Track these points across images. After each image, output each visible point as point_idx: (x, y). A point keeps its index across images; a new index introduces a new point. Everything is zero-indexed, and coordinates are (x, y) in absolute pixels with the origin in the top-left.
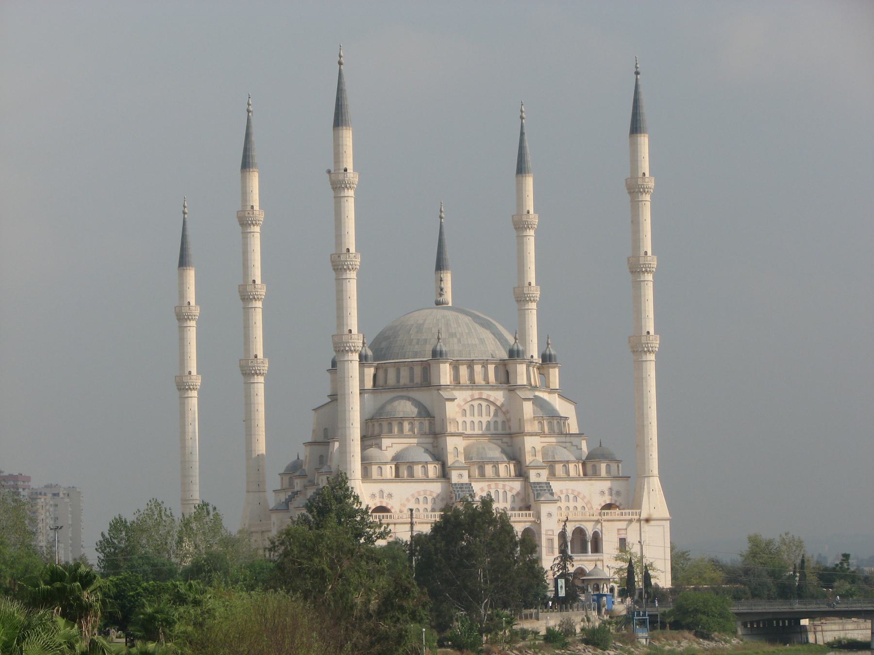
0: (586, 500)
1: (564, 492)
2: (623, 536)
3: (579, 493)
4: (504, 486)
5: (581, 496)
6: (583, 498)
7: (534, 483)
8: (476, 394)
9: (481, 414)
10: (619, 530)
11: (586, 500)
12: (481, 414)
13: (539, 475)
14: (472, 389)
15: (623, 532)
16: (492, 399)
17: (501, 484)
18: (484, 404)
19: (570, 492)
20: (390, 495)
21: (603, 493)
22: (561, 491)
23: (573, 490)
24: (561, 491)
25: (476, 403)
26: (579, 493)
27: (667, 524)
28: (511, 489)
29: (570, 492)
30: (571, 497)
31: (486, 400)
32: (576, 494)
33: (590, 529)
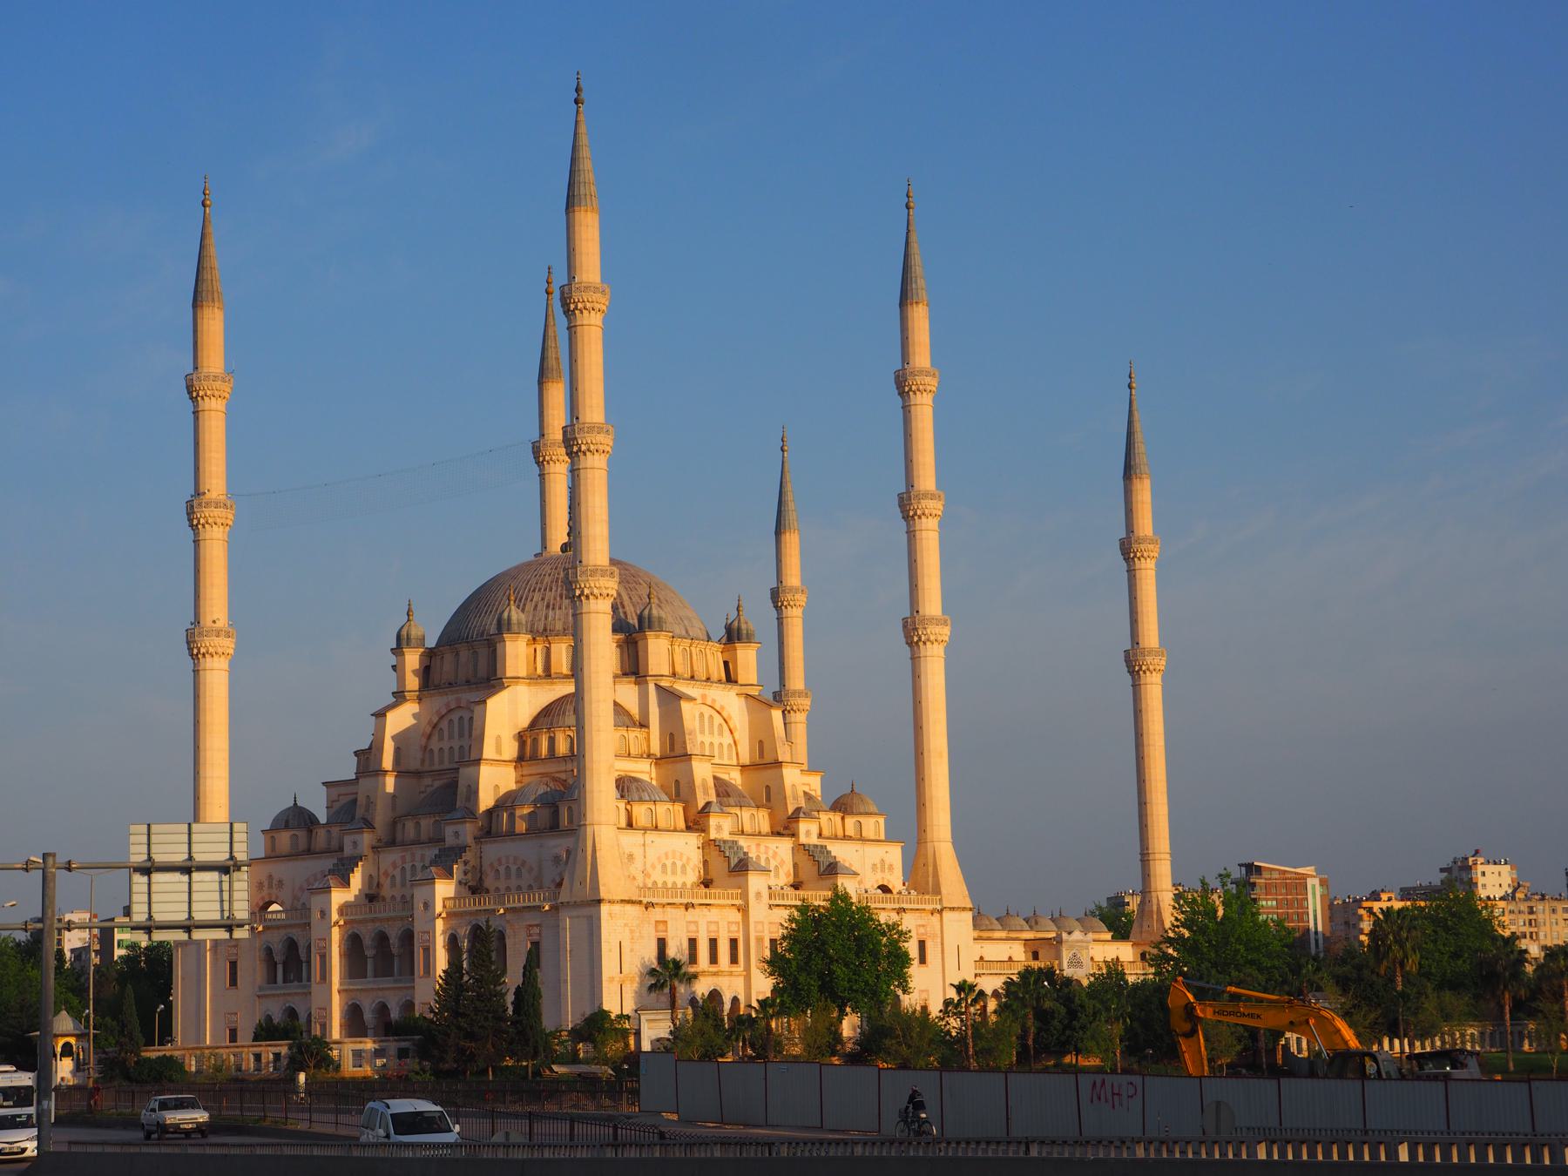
2: (536, 938)
4: (423, 856)
6: (531, 869)
12: (461, 735)
17: (418, 851)
21: (557, 859)
22: (499, 860)
23: (515, 858)
24: (499, 860)
25: (455, 717)
26: (523, 863)
30: (514, 868)
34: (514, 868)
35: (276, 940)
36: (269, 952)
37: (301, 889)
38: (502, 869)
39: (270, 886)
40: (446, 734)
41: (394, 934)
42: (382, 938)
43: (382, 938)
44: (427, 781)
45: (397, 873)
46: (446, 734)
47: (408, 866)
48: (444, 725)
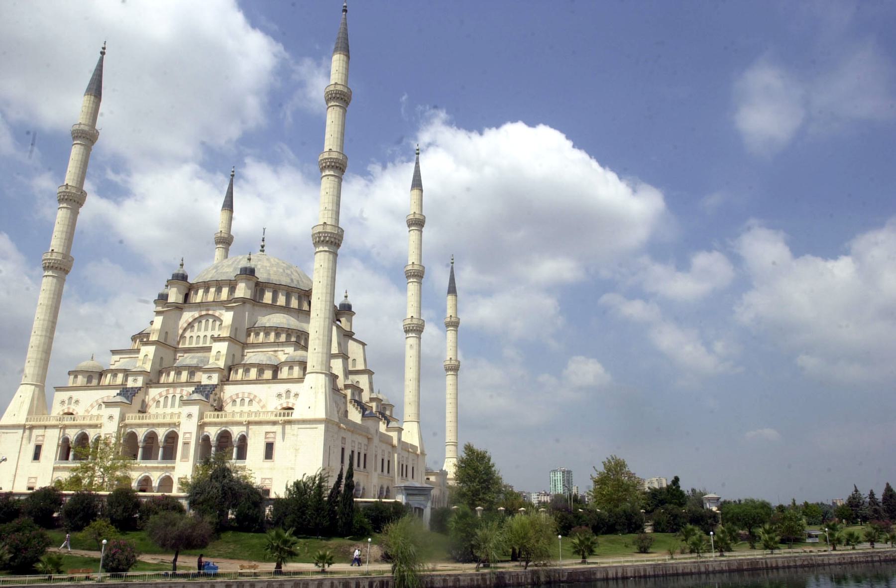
0: (261, 404)
1: (240, 396)
2: (270, 440)
3: (255, 396)
5: (257, 400)
7: (206, 385)
10: (267, 433)
11: (261, 404)
15: (272, 435)
19: (246, 395)
20: (77, 402)
21: (279, 395)
24: (237, 395)
26: (255, 396)
27: (322, 427)
29: (246, 395)
30: (247, 400)
32: (252, 397)
33: (236, 432)
34: (247, 400)
35: (72, 434)
36: (66, 441)
37: (92, 406)
38: (238, 401)
39: (70, 403)
41: (161, 433)
42: (151, 438)
43: (151, 438)
45: (162, 400)
47: (170, 396)
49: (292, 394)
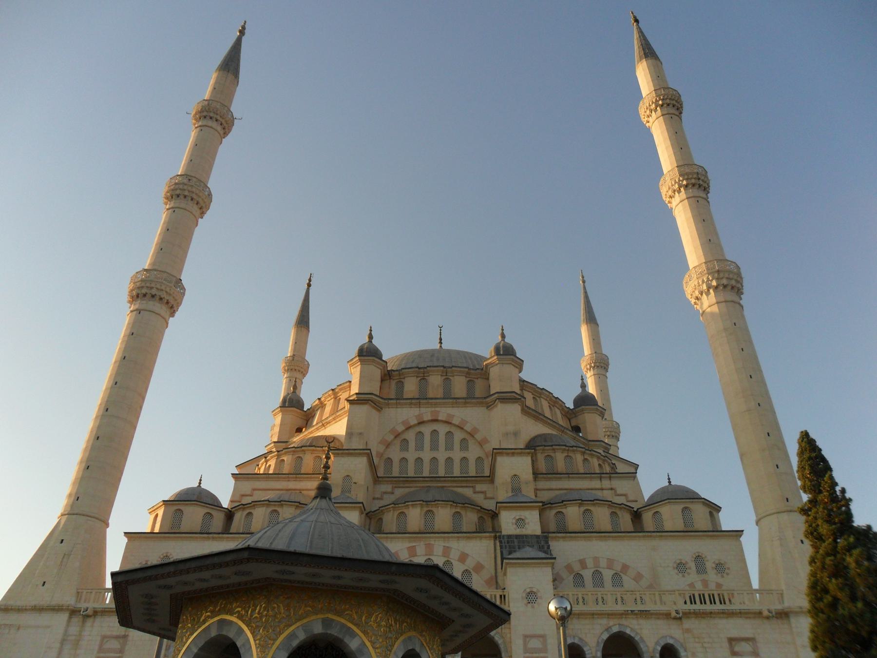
1: (590, 563)
3: (625, 568)
4: (446, 551)
6: (638, 577)
7: (509, 536)
8: (427, 413)
9: (434, 446)
10: (731, 641)
12: (434, 446)
13: (520, 522)
14: (419, 405)
16: (456, 421)
18: (442, 429)
19: (603, 563)
21: (681, 567)
23: (610, 563)
25: (427, 430)
28: (463, 558)
30: (607, 575)
31: (447, 423)
40: (412, 445)
44: (386, 487)
46: (412, 445)
48: (411, 436)
49: (709, 565)
